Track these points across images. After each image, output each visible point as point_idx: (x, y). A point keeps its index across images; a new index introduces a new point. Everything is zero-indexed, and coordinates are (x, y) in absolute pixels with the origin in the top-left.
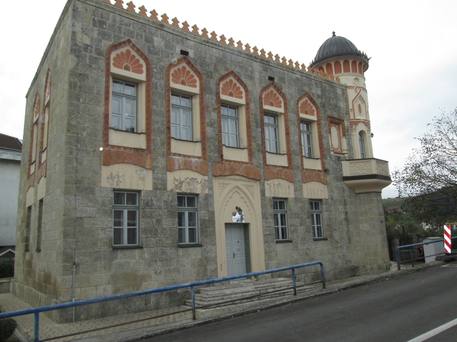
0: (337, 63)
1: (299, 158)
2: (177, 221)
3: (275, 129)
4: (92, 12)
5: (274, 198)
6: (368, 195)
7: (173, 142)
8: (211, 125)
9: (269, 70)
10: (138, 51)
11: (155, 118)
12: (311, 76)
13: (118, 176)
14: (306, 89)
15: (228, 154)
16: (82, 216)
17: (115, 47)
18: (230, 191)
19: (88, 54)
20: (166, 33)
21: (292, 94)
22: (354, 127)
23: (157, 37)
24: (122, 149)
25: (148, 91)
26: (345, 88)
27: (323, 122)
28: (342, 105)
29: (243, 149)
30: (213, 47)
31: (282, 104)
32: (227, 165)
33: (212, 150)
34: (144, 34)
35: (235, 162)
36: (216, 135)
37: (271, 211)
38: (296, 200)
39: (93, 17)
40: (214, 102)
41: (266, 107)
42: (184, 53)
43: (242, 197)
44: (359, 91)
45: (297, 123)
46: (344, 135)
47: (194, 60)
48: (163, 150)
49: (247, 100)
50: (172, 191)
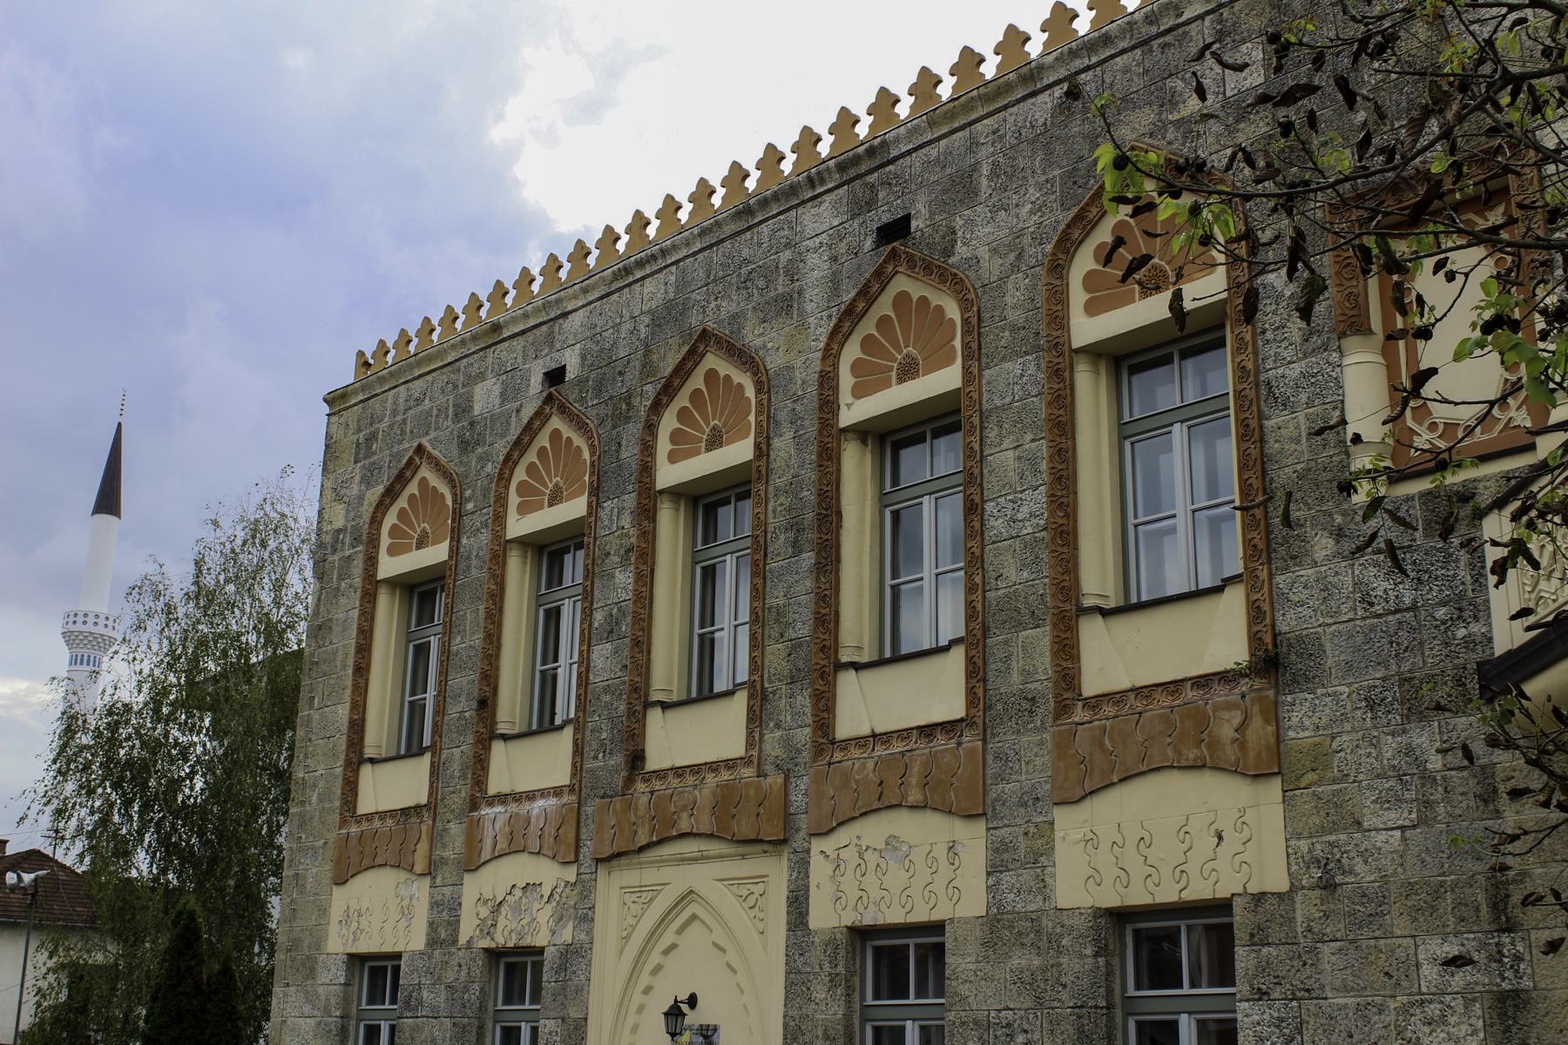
33: (602, 744)
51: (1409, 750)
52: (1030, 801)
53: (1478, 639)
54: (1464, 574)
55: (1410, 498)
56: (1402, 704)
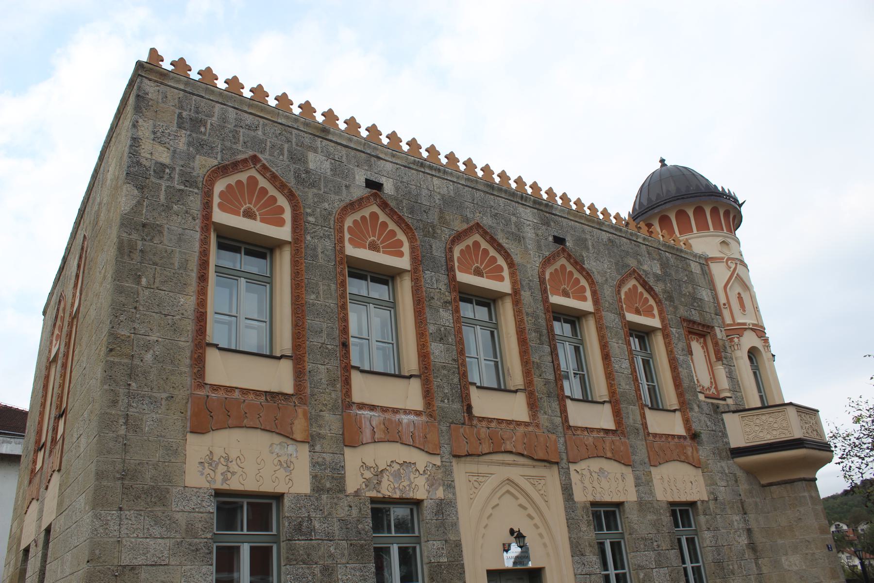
0: (681, 214)
1: (636, 409)
2: (373, 570)
3: (577, 349)
4: (176, 101)
5: (594, 504)
6: (788, 486)
7: (356, 378)
8: (442, 339)
9: (552, 224)
10: (274, 179)
11: (312, 321)
12: (637, 237)
13: (227, 459)
14: (632, 263)
15: (484, 405)
16: (135, 562)
17: (223, 170)
18: (494, 491)
19: (164, 184)
20: (333, 144)
21: (606, 272)
22: (736, 340)
23: (316, 151)
24: (237, 394)
25: (295, 263)
26: (705, 261)
27: (674, 330)
28: (705, 294)
29: (516, 392)
30: (433, 175)
31: (588, 294)
32: (483, 430)
33: (445, 395)
34: (286, 146)
35: (500, 421)
36: (454, 360)
37: (588, 534)
38: (643, 505)
39: (177, 111)
40: (443, 288)
41: (556, 299)
42: (373, 185)
43: (521, 506)
44: (733, 266)
45: (622, 332)
46: (719, 359)
47: (396, 199)
48: (333, 396)
49: (514, 283)
50: (357, 494)
51: (722, 467)
52: (643, 463)
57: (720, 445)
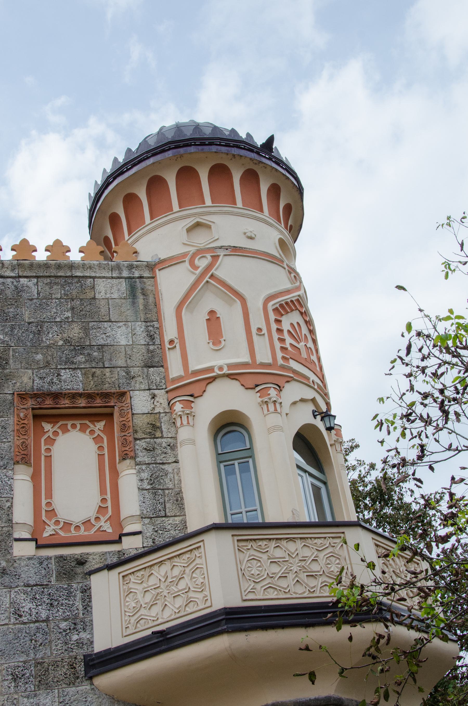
22: (178, 407)
53: (85, 642)
54: (79, 604)
55: (48, 558)
56: (35, 678)
57: (54, 651)
